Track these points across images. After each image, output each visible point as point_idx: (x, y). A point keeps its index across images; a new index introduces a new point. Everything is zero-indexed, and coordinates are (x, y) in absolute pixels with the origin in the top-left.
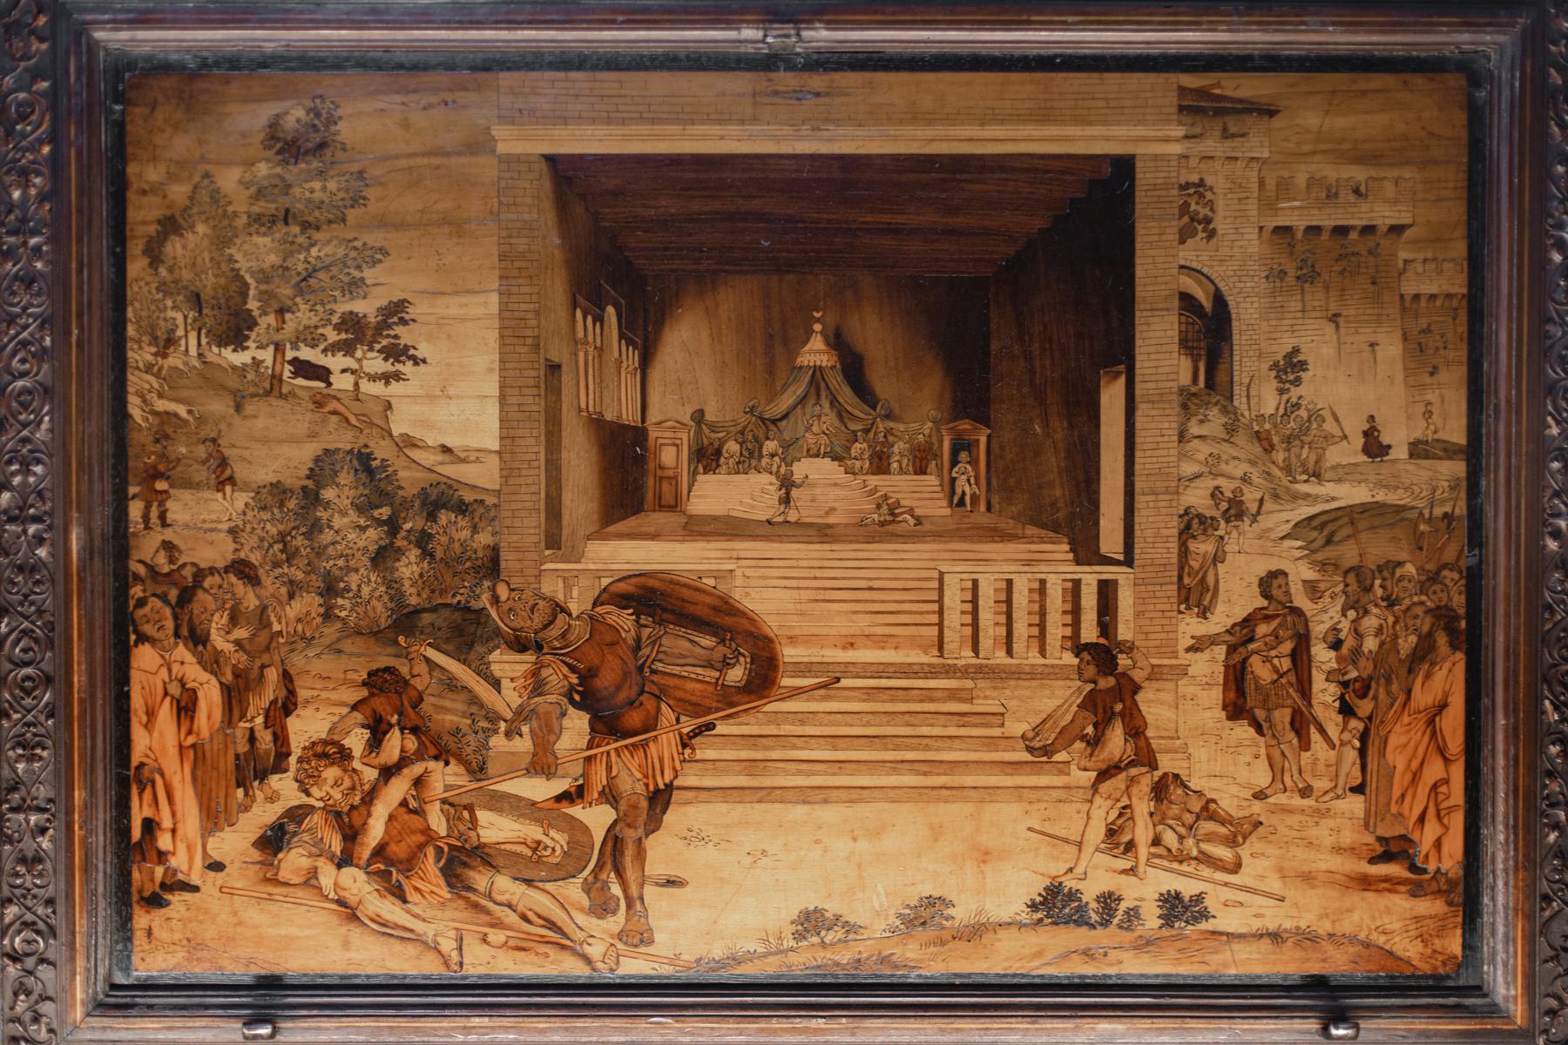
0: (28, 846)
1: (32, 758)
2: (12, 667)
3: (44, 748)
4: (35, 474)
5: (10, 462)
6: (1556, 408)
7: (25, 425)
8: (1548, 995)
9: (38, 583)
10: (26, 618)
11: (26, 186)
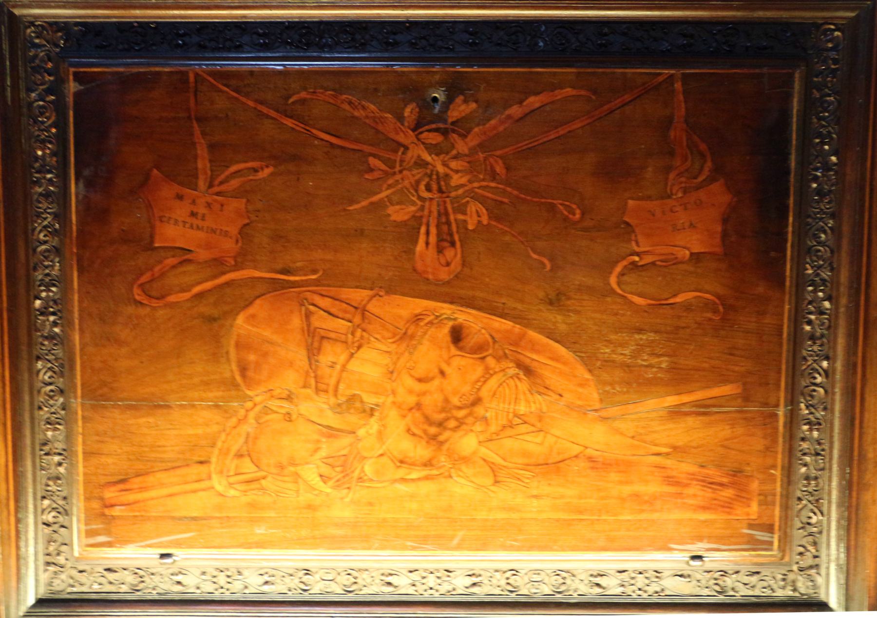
0: (53, 471)
1: (56, 429)
2: (43, 385)
3: (60, 424)
4: (52, 292)
5: (40, 286)
6: (811, 259)
7: (47, 267)
8: (800, 546)
9: (55, 345)
10: (49, 361)
11: (43, 150)
